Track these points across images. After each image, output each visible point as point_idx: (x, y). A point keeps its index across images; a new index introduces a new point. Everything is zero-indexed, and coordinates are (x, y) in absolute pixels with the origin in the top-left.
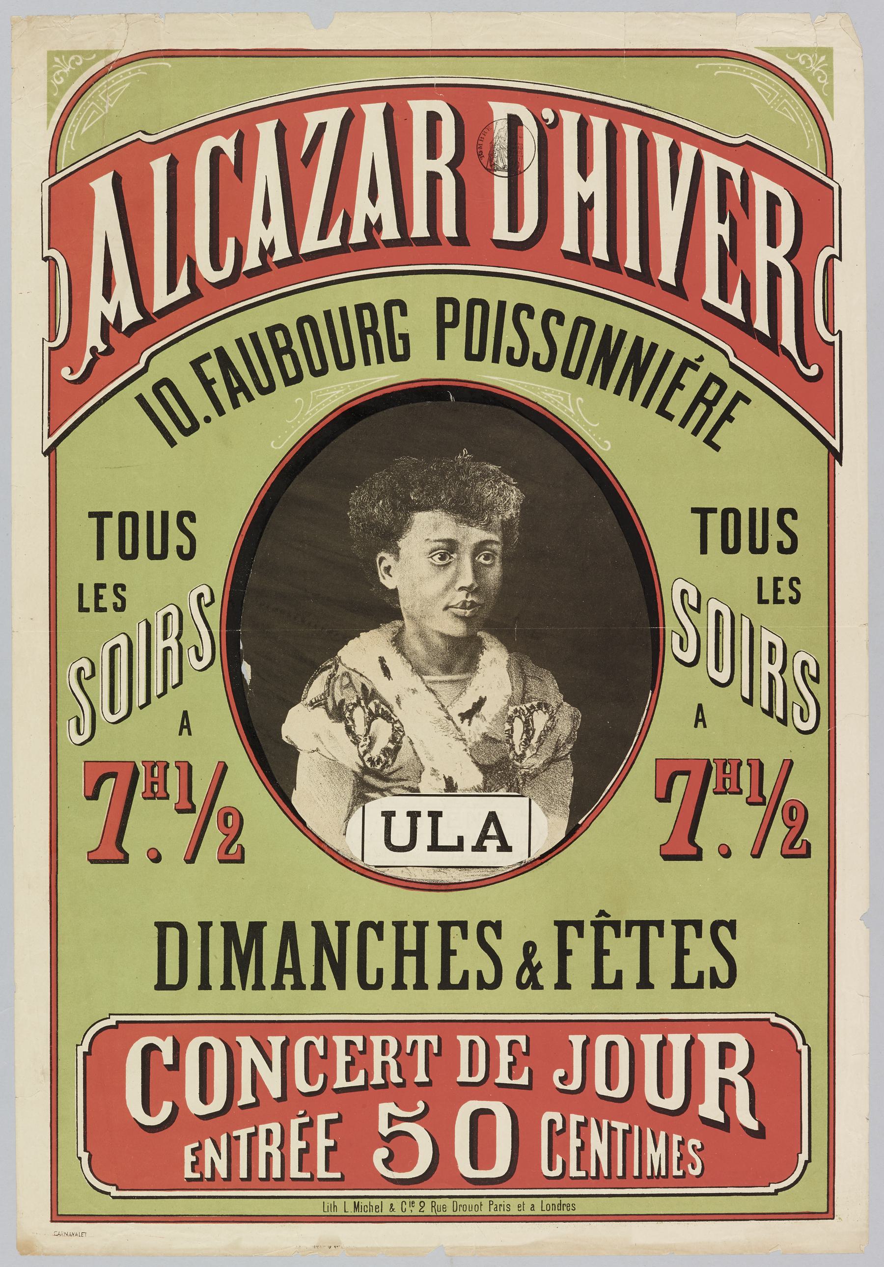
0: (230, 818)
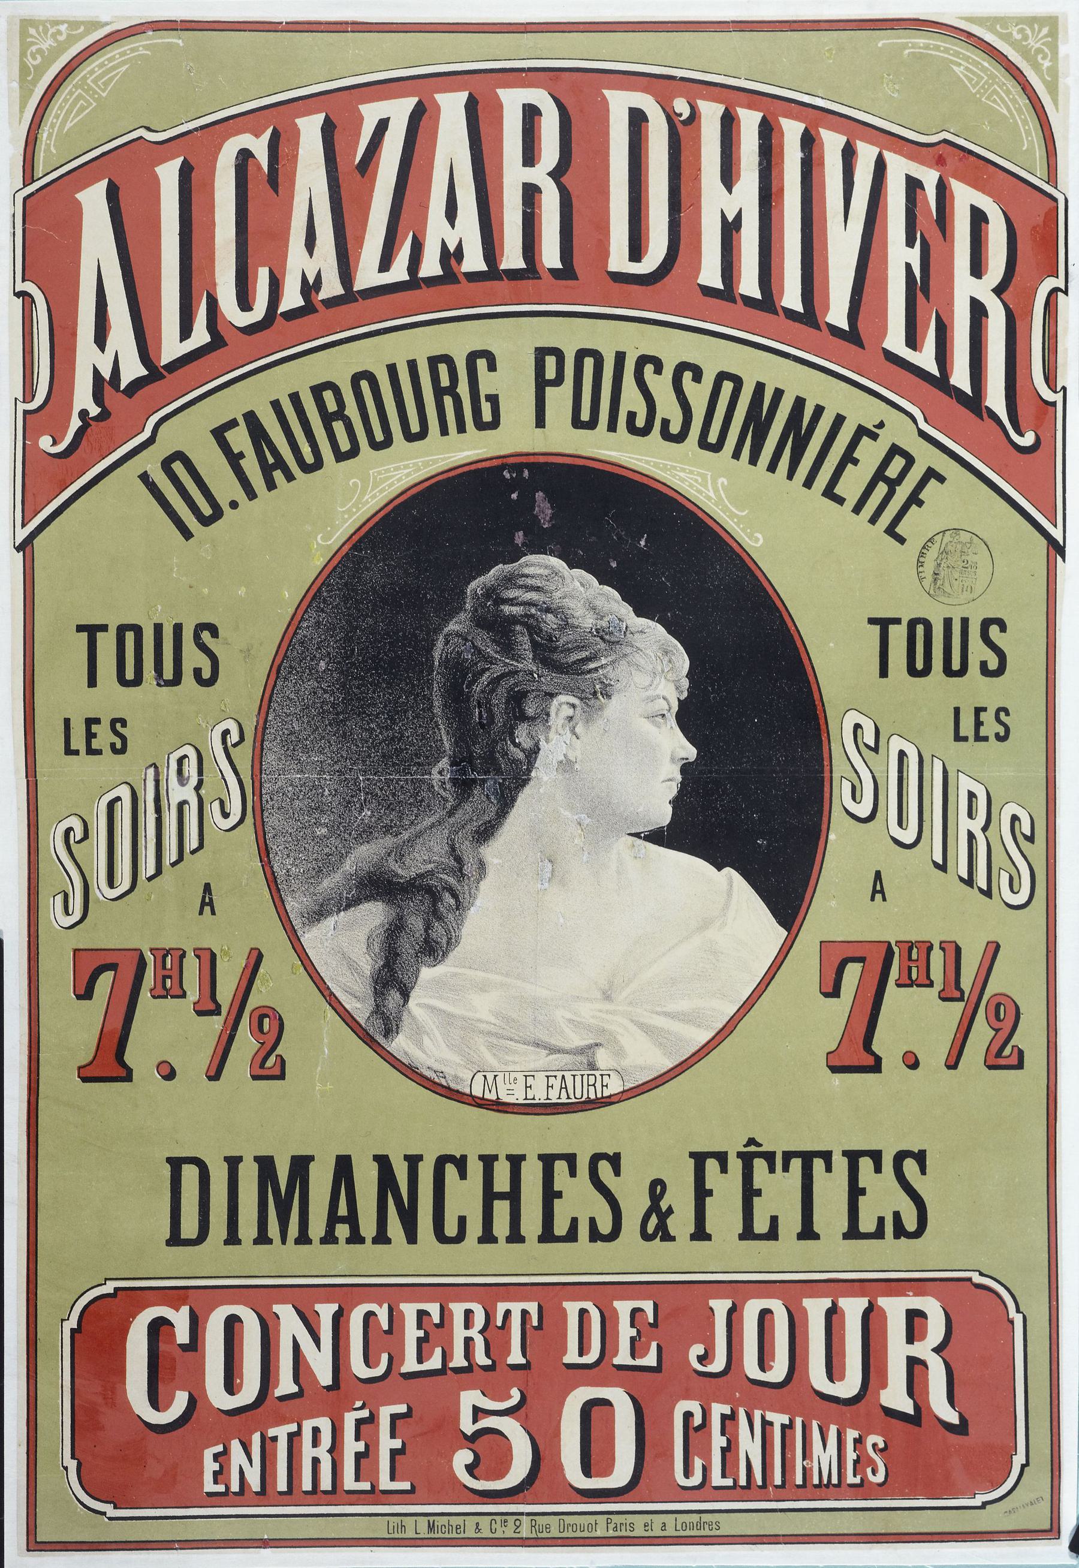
0: (266, 1021)
